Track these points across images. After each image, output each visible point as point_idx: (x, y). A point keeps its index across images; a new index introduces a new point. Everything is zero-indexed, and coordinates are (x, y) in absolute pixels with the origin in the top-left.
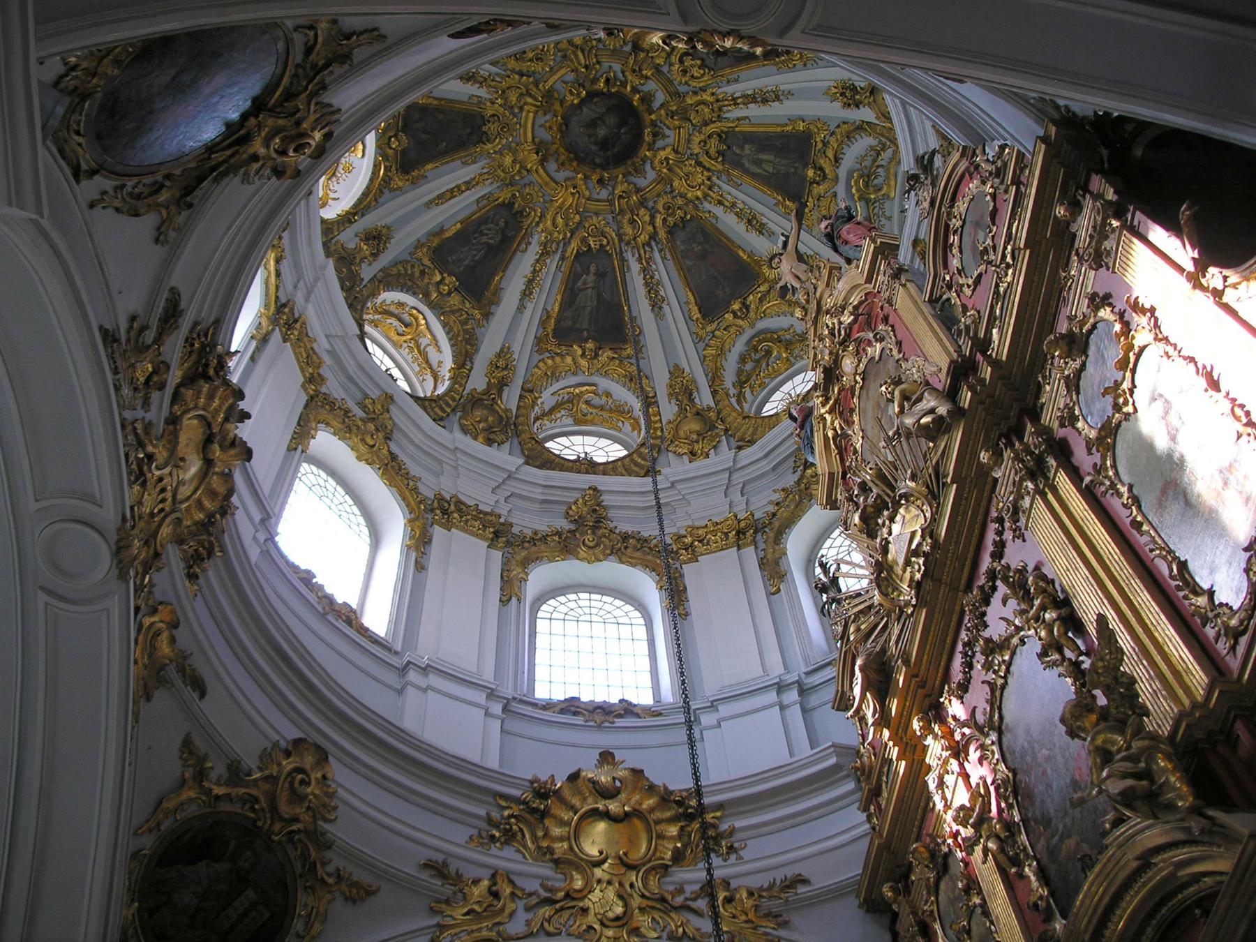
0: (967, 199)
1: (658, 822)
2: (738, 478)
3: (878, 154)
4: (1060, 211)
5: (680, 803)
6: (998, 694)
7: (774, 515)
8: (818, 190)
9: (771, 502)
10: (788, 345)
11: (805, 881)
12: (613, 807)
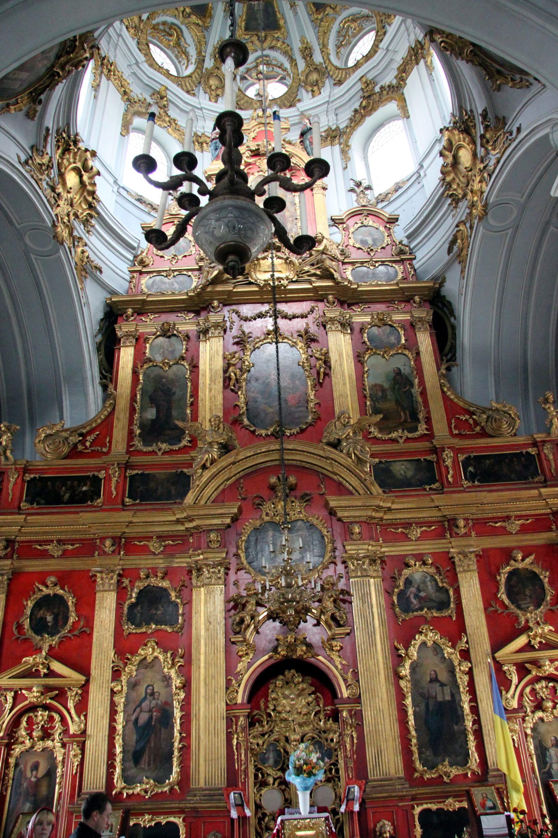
0: (375, 225)
1: (85, 197)
2: (135, 68)
3: (280, 68)
4: (417, 299)
5: (94, 198)
6: (265, 341)
7: (135, 102)
8: (255, 38)
9: (137, 96)
10: (178, 44)
11: (101, 272)
12: (85, 178)
